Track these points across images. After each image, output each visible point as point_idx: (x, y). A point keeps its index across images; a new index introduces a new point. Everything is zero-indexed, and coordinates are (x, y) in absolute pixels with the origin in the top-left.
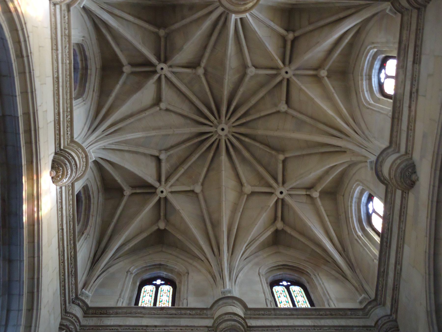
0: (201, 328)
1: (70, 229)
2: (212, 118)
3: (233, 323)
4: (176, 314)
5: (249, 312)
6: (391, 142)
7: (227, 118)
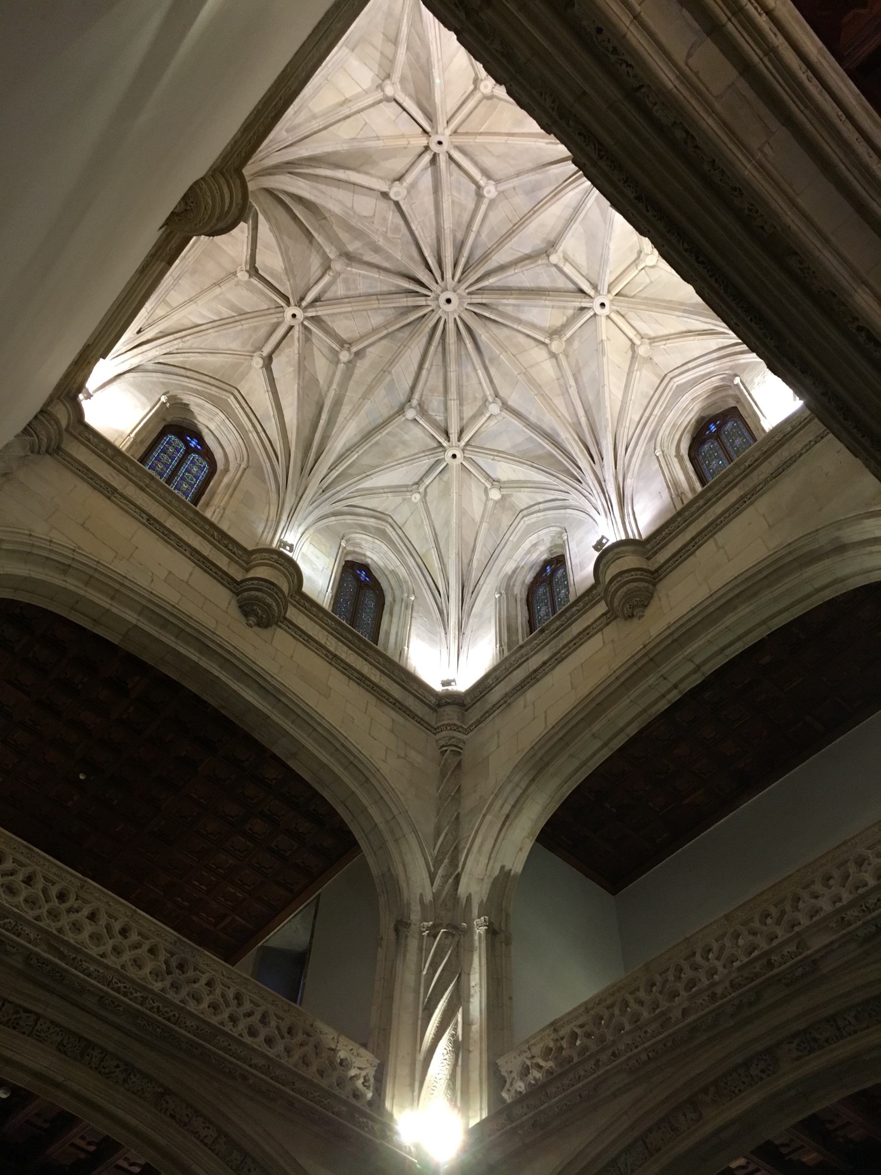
0: (598, 623)
1: (350, 642)
3: (625, 589)
4: (562, 625)
5: (648, 546)
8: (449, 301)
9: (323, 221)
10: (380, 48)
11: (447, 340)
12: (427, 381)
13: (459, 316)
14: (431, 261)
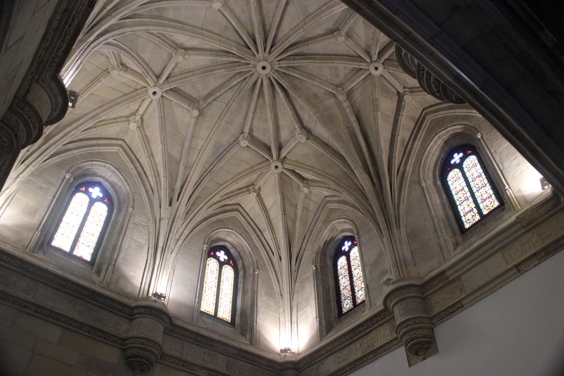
2: (284, 64)
6: (175, 326)
7: (272, 78)
8: (264, 68)
9: (349, 126)
10: (311, 202)
11: (262, 36)
12: (277, 7)
13: (254, 56)
14: (278, 90)
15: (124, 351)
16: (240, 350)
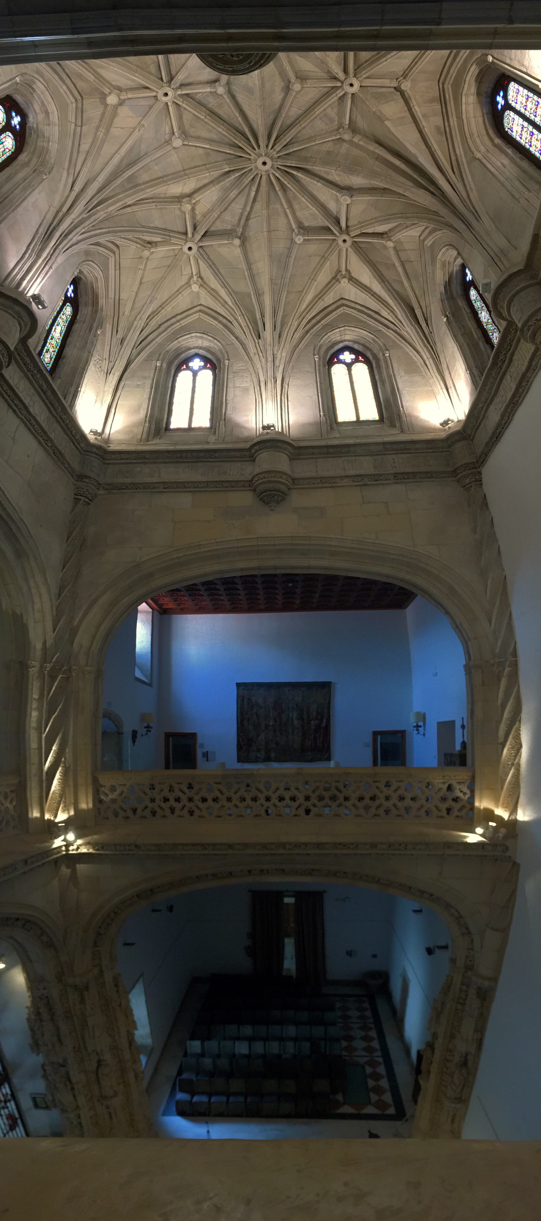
15: (254, 490)
16: (384, 443)
